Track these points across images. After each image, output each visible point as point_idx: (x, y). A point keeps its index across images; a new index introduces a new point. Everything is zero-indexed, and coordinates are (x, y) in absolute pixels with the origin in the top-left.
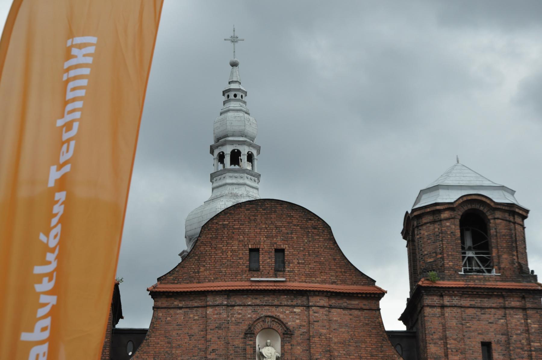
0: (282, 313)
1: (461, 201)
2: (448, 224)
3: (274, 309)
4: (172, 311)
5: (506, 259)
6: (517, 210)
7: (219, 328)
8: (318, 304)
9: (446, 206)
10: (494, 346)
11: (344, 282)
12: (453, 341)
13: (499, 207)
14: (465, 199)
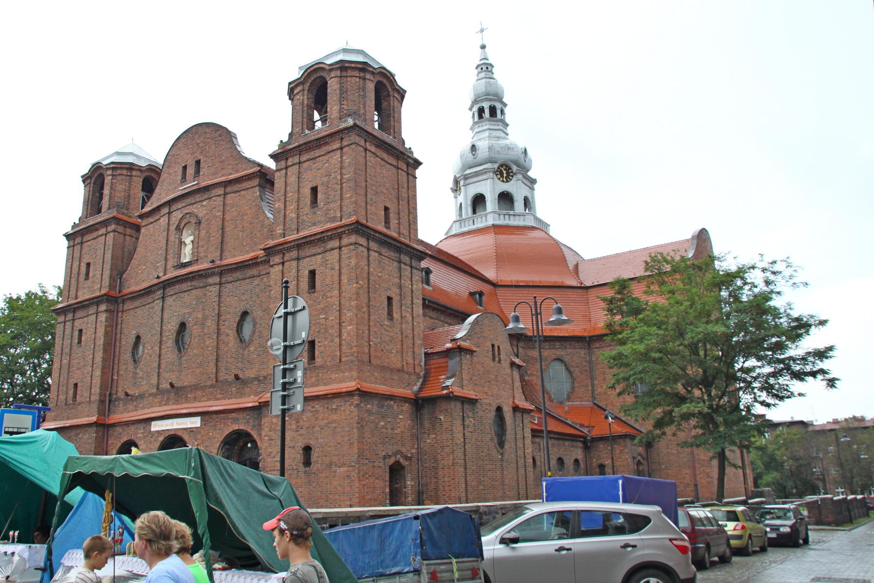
0: (196, 208)
1: (306, 73)
2: (298, 97)
3: (191, 207)
4: (148, 227)
5: (335, 110)
6: (346, 65)
7: (164, 231)
8: (217, 194)
9: (296, 83)
10: (319, 189)
11: (237, 171)
12: (291, 194)
13: (331, 67)
14: (309, 71)
